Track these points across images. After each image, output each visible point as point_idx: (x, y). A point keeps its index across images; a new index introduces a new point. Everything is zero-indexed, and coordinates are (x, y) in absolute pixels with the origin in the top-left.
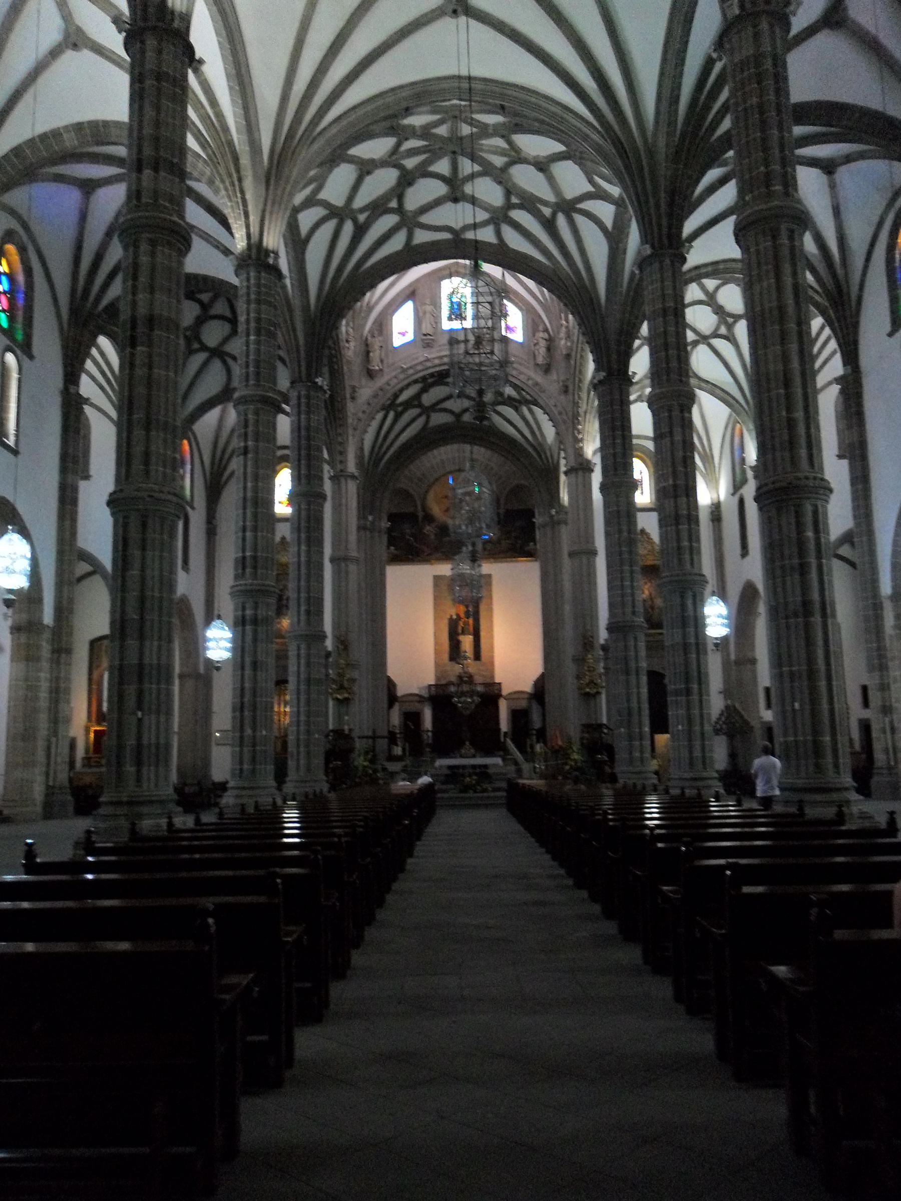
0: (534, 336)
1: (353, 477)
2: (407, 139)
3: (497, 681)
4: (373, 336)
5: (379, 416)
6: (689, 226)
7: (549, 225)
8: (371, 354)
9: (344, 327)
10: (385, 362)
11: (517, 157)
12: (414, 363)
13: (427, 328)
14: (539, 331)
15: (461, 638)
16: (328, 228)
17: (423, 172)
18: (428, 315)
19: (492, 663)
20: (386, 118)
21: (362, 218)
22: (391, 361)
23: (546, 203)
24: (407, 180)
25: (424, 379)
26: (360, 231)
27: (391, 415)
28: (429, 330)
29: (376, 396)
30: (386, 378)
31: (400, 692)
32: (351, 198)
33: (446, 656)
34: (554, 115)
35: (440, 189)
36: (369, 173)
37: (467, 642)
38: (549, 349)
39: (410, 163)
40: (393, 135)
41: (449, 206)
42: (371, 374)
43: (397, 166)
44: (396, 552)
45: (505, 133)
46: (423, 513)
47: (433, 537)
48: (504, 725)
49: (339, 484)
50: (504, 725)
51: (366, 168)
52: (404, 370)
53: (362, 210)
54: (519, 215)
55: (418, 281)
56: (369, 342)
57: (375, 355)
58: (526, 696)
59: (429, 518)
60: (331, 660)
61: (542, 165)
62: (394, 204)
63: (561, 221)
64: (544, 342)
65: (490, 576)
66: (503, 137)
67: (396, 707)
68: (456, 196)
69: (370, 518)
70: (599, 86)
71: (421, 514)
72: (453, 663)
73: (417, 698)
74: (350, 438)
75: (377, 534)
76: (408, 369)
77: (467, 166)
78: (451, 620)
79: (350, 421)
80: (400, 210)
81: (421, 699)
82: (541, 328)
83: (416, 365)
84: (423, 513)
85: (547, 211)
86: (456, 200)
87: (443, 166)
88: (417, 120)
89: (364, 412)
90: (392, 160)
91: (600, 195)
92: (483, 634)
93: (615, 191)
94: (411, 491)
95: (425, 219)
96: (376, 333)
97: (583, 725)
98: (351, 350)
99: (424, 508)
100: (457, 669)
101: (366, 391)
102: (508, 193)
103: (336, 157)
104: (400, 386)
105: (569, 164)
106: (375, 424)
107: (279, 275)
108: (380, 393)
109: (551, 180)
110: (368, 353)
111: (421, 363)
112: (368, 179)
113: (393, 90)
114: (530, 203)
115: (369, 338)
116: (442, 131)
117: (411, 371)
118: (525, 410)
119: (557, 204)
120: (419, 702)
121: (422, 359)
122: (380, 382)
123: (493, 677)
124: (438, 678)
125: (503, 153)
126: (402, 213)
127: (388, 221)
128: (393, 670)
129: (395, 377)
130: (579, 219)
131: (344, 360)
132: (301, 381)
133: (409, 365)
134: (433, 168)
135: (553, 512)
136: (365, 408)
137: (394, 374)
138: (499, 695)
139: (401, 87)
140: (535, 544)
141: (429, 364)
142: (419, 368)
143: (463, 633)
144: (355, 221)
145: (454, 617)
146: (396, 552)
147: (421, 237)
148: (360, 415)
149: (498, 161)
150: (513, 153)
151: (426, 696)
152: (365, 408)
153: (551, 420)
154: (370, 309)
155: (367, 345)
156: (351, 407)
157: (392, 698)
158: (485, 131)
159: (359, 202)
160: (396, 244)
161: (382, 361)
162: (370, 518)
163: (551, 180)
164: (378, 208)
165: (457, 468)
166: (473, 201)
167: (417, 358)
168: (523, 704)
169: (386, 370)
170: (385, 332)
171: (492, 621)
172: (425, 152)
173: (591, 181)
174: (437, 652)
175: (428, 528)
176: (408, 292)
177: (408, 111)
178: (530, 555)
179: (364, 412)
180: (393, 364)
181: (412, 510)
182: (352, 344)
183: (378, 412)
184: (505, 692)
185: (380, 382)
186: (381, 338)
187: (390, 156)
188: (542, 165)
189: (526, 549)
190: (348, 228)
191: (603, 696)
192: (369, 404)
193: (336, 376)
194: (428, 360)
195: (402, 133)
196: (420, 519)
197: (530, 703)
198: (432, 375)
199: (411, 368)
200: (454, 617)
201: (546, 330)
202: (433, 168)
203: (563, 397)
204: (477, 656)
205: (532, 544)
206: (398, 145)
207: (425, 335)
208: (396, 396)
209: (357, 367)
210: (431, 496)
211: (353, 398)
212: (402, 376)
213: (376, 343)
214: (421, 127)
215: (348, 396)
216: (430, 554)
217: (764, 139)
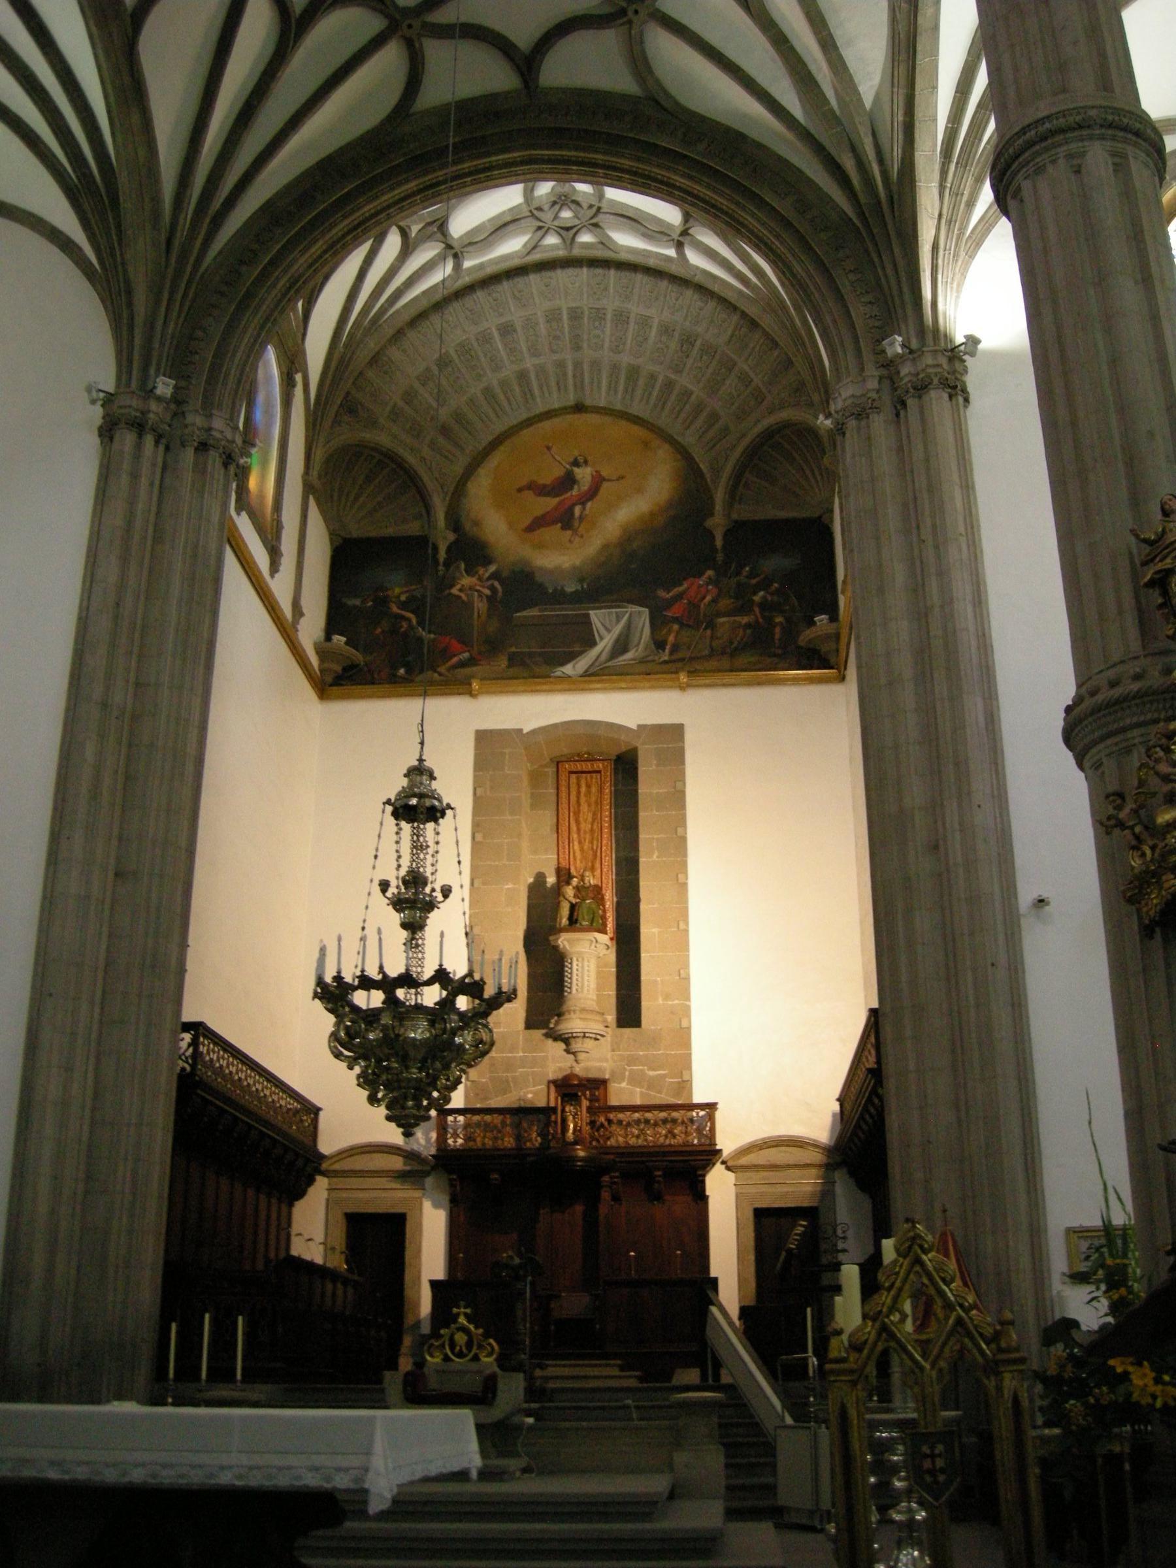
15: (564, 941)
19: (683, 1037)
44: (358, 657)
46: (451, 537)
58: (817, 1157)
65: (677, 731)
67: (320, 1189)
71: (444, 539)
72: (538, 1034)
73: (397, 1163)
78: (537, 888)
84: (451, 537)
92: (649, 931)
94: (411, 459)
99: (455, 524)
120: (402, 1176)
123: (685, 1085)
138: (709, 1155)
140: (834, 618)
145: (551, 880)
146: (358, 657)
165: (571, 400)
171: (683, 887)
175: (467, 581)
181: (413, 528)
184: (727, 1142)
189: (806, 636)
196: (442, 555)
197: (827, 1192)
205: (822, 619)
210: (480, 489)
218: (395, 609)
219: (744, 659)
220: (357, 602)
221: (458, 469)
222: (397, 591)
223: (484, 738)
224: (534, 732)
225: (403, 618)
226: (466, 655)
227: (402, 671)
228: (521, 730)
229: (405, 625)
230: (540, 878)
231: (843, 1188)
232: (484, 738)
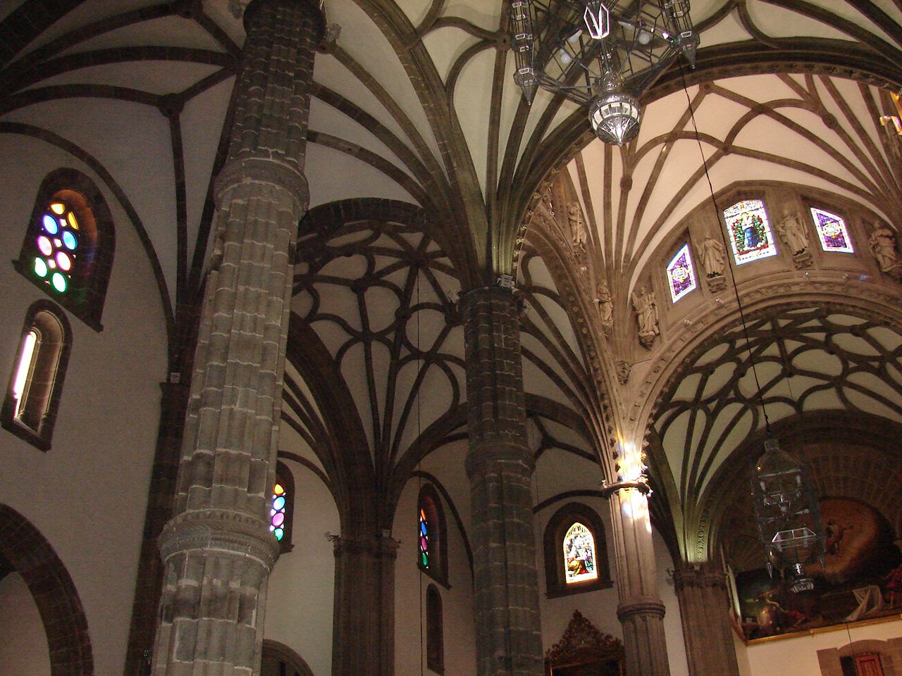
0: (870, 236)
4: (640, 295)
8: (641, 317)
10: (662, 324)
13: (713, 265)
14: (874, 230)
18: (710, 252)
22: (670, 320)
30: (667, 343)
55: (689, 216)
56: (635, 303)
64: (888, 240)
75: (710, 589)
76: (696, 324)
82: (877, 225)
83: (705, 316)
110: (637, 316)
111: (712, 312)
117: (700, 327)
121: (713, 307)
133: (694, 320)
141: (724, 312)
142: (712, 319)
155: (634, 309)
167: (705, 309)
169: (665, 334)
170: (656, 287)
176: (678, 233)
194: (721, 307)
201: (884, 225)
207: (714, 274)
211: (625, 381)
212: (689, 336)
218: (769, 601)
220: (752, 600)
222: (767, 593)
223: (821, 654)
224: (843, 648)
225: (774, 605)
226: (804, 618)
227: (778, 629)
228: (836, 648)
229: (774, 608)
232: (821, 654)
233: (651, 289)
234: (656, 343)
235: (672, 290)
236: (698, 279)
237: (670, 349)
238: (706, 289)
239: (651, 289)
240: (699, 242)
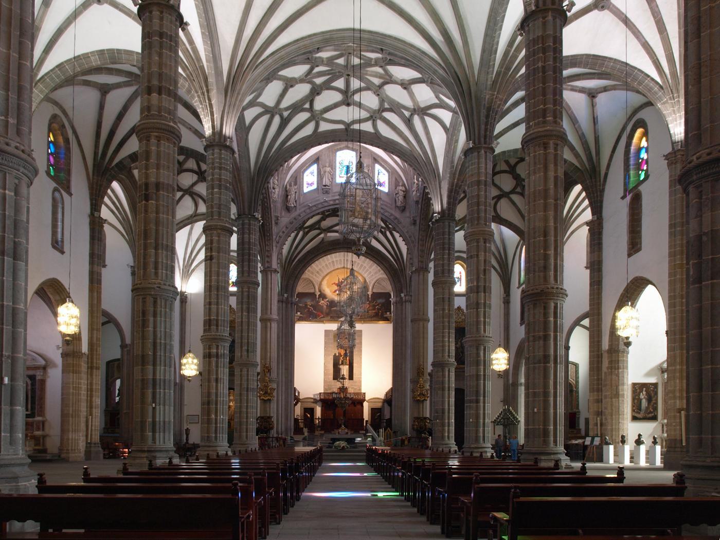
1: (275, 271)
2: (317, 66)
3: (363, 391)
4: (290, 185)
5: (293, 235)
6: (499, 127)
7: (409, 122)
9: (274, 181)
11: (389, 80)
12: (317, 203)
13: (326, 181)
16: (264, 120)
17: (327, 86)
18: (327, 174)
20: (304, 53)
21: (286, 114)
23: (407, 109)
24: (316, 91)
25: (323, 213)
26: (284, 123)
27: (301, 233)
28: (328, 183)
29: (291, 223)
30: (298, 212)
31: (301, 397)
32: (279, 102)
33: (331, 377)
34: (415, 56)
35: (337, 97)
36: (292, 86)
37: (345, 370)
38: (405, 197)
39: (319, 81)
40: (307, 63)
41: (344, 108)
42: (288, 209)
43: (310, 82)
45: (383, 64)
47: (325, 307)
48: (366, 415)
49: (267, 275)
50: (366, 415)
51: (289, 83)
52: (310, 208)
53: (287, 109)
54: (389, 115)
57: (292, 197)
58: (382, 401)
59: (322, 296)
60: (259, 377)
61: (406, 85)
62: (307, 106)
63: (417, 121)
66: (381, 67)
67: (299, 404)
68: (347, 99)
69: (286, 295)
70: (444, 38)
73: (312, 400)
74: (274, 248)
77: (355, 83)
79: (274, 237)
80: (311, 109)
81: (315, 401)
85: (407, 114)
86: (348, 105)
87: (340, 83)
88: (324, 55)
89: (283, 232)
90: (306, 78)
91: (442, 105)
93: (452, 103)
95: (327, 115)
96: (293, 183)
97: (415, 418)
98: (276, 194)
99: (320, 291)
100: (336, 386)
101: (285, 219)
102: (382, 101)
103: (271, 76)
104: (306, 218)
105: (423, 86)
106: (290, 239)
107: (233, 152)
108: (294, 221)
109: (412, 95)
110: (287, 196)
111: (321, 203)
112: (291, 90)
113: (310, 36)
114: (396, 108)
115: (288, 186)
116: (341, 61)
117: (314, 208)
118: (388, 234)
119: (414, 109)
122: (294, 214)
123: (360, 390)
124: (325, 389)
125: (380, 77)
126: (312, 111)
127: (302, 116)
128: (297, 385)
129: (304, 211)
130: (427, 119)
131: (271, 200)
132: (244, 214)
134: (335, 84)
135: (402, 295)
136: (284, 229)
137: (303, 210)
139: (315, 35)
142: (320, 206)
143: (342, 364)
144: (281, 116)
147: (324, 127)
148: (281, 234)
149: (377, 81)
150: (388, 77)
151: (319, 399)
152: (284, 229)
153: (404, 240)
154: (290, 168)
156: (275, 229)
157: (297, 400)
158: (369, 63)
159: (284, 105)
160: (308, 130)
161: (296, 201)
162: (286, 295)
163: (412, 95)
164: (296, 108)
165: (342, 266)
166: (360, 105)
168: (379, 405)
169: (298, 206)
172: (328, 74)
173: (437, 97)
174: (325, 374)
175: (322, 302)
177: (319, 50)
178: (387, 319)
179: (283, 232)
180: (303, 203)
181: (312, 291)
182: (277, 190)
183: (293, 232)
184: (367, 398)
185: (294, 214)
186: (296, 187)
187: (306, 76)
188: (406, 85)
189: (385, 316)
190: (277, 120)
191: (428, 402)
192: (287, 228)
193: (266, 210)
194: (326, 201)
195: (314, 63)
197: (383, 404)
198: (328, 211)
199: (315, 206)
200: (337, 354)
202: (335, 84)
203: (413, 227)
204: (351, 377)
205: (388, 313)
206: (312, 69)
208: (305, 222)
209: (279, 205)
211: (276, 223)
212: (308, 211)
213: (293, 189)
214: (327, 58)
215: (273, 222)
216: (323, 317)
217: (544, 89)
219: (375, 318)
221: (320, 279)
230: (335, 354)
231: (386, 405)
233: (296, 184)
234: (294, 210)
235: (305, 185)
236: (318, 184)
237: (299, 215)
238: (320, 191)
239: (296, 184)
240: (322, 168)
